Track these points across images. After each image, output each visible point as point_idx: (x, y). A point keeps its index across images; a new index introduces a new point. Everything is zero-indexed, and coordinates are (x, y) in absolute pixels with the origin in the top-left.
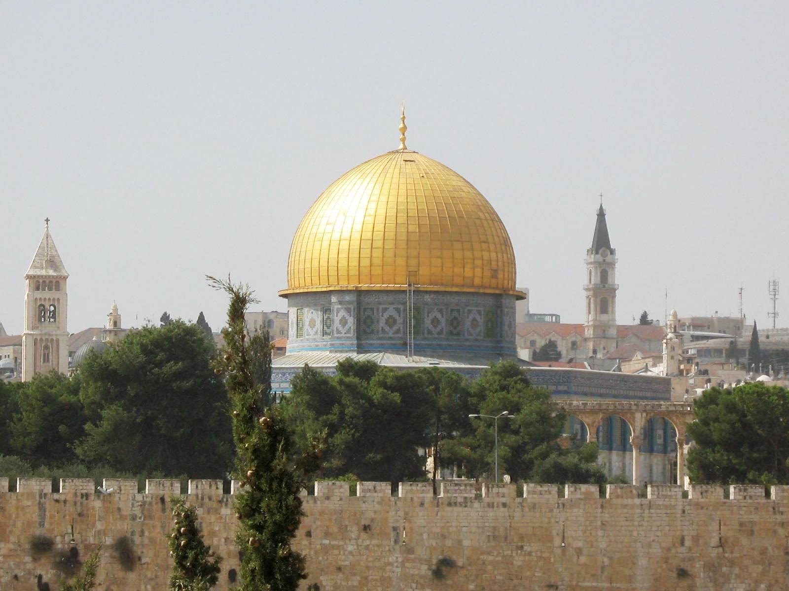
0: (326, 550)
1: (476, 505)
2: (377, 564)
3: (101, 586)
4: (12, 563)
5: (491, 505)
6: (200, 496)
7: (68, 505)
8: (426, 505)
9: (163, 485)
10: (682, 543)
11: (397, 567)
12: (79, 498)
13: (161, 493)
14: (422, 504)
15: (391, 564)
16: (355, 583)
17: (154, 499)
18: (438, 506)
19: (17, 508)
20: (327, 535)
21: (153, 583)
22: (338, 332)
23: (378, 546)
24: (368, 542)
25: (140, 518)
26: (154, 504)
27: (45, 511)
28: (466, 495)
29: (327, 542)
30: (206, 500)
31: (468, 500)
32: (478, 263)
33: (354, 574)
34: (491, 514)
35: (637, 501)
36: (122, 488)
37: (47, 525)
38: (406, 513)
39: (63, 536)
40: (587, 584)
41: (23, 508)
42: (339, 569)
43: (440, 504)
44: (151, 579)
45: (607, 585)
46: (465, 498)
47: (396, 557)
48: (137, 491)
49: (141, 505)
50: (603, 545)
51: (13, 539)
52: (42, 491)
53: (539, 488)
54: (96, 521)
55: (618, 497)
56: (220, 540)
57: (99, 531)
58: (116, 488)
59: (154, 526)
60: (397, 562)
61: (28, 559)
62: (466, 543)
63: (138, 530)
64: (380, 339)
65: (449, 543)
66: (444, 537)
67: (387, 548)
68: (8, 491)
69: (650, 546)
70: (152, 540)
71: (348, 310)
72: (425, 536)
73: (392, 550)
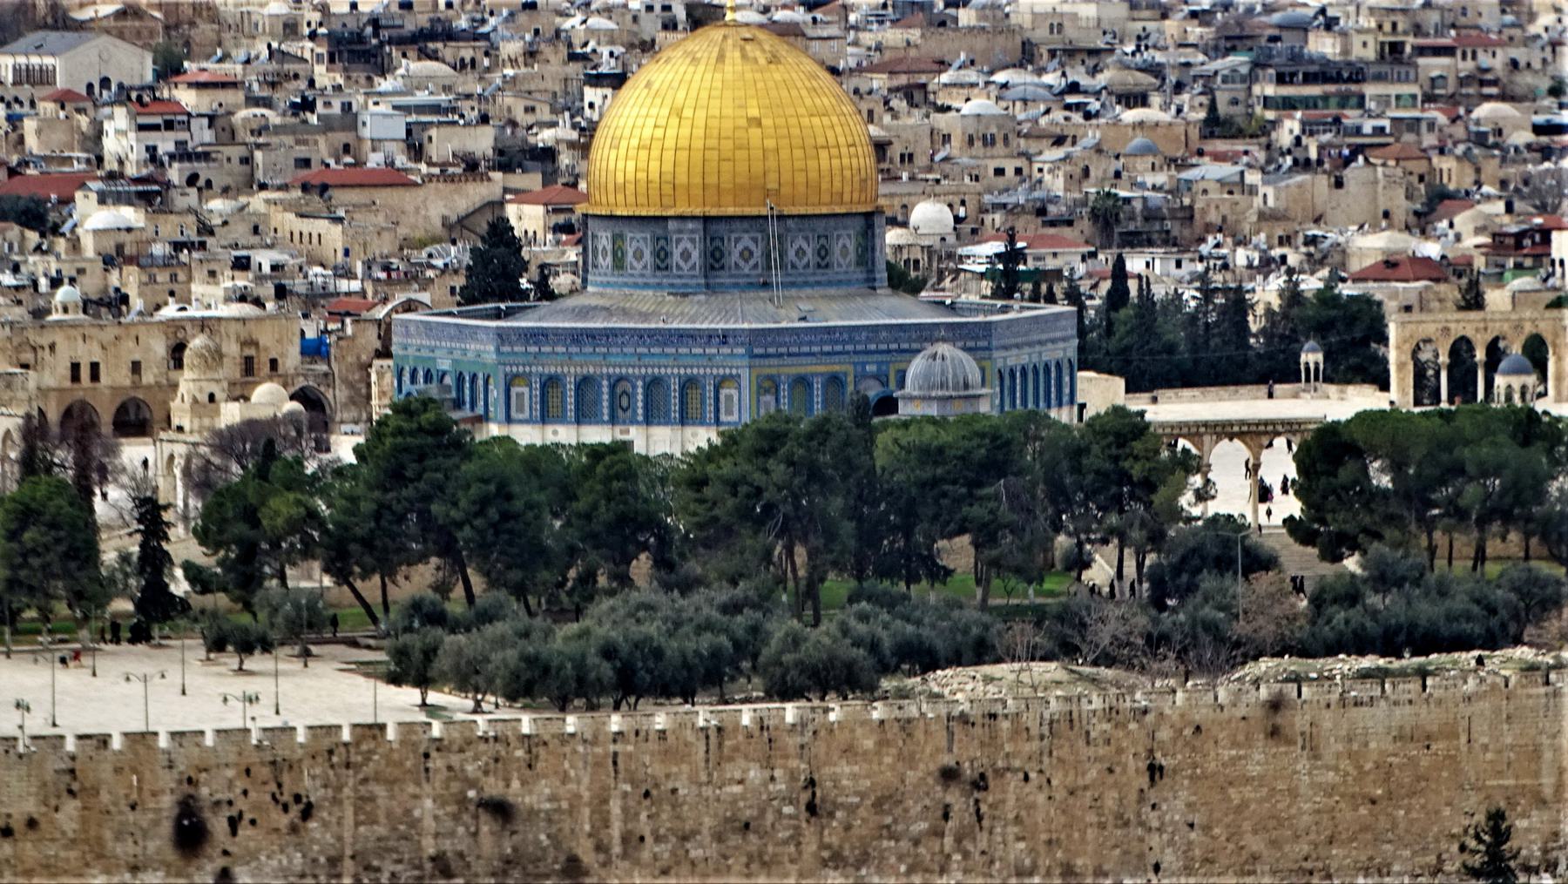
0: (1234, 760)
1: (1383, 703)
5: (1396, 703)
14: (1328, 706)
20: (1235, 744)
22: (679, 268)
29: (1234, 752)
34: (1398, 711)
35: (1542, 690)
40: (1494, 783)
47: (1303, 765)
50: (1509, 740)
51: (922, 766)
55: (1523, 687)
57: (1007, 755)
61: (939, 788)
62: (1373, 745)
64: (731, 276)
65: (1355, 747)
66: (1350, 740)
70: (1060, 760)
71: (693, 241)
72: (1332, 740)
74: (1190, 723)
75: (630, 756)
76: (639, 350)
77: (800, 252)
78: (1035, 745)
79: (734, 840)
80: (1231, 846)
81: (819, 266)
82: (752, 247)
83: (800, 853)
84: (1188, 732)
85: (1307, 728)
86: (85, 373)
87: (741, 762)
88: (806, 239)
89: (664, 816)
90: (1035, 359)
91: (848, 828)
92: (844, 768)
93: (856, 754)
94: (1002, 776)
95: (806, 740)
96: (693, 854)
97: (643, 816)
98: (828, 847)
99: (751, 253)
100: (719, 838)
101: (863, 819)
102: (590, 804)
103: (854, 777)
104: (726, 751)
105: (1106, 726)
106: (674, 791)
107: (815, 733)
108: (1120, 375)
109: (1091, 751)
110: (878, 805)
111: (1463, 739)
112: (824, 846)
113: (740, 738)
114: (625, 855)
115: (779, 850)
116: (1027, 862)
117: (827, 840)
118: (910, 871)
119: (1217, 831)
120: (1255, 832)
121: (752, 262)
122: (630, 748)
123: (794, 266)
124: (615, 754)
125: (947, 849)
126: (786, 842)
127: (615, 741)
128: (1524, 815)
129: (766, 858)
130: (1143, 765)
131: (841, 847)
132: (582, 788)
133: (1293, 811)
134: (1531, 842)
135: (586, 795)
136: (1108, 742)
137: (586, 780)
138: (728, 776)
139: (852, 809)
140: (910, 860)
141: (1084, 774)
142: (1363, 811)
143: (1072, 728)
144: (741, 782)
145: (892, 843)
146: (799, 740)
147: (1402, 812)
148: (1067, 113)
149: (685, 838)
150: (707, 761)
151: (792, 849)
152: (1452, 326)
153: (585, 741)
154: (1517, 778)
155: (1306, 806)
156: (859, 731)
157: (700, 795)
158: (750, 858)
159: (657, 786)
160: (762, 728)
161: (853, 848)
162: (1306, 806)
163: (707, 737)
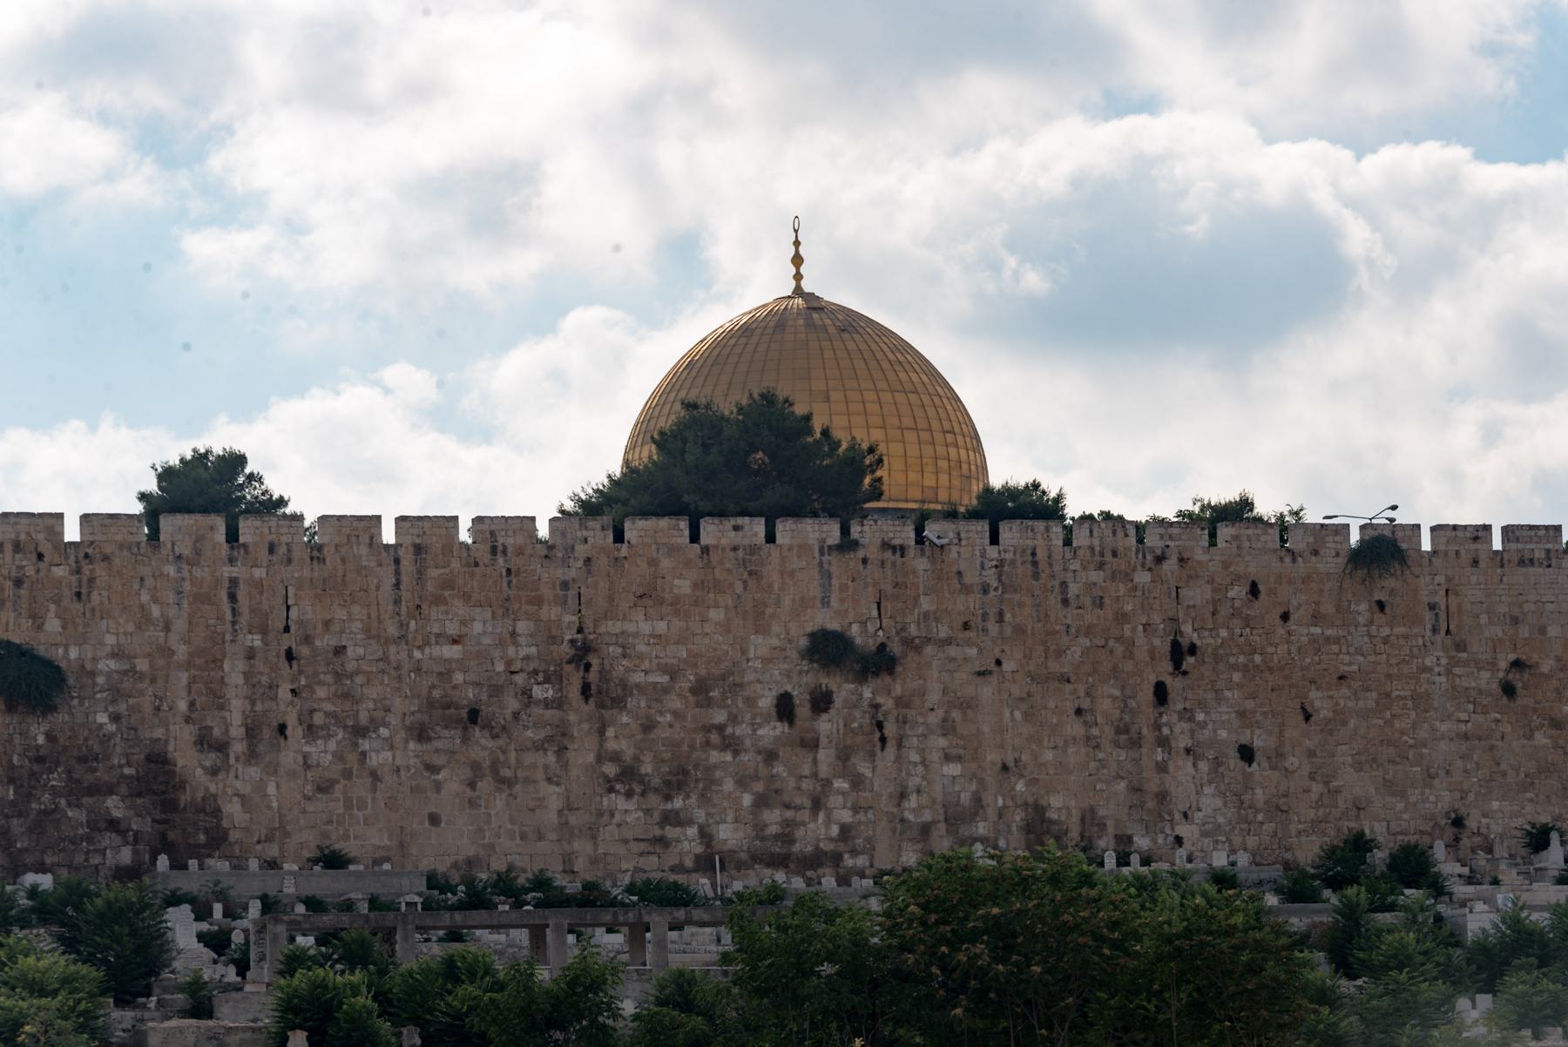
0: (1317, 644)
2: (1406, 669)
3: (933, 713)
4: (777, 672)
6: (1097, 549)
7: (869, 567)
8: (1482, 564)
9: (1032, 530)
11: (1439, 674)
13: (1030, 542)
14: (1475, 562)
15: (1430, 670)
16: (1371, 704)
17: (1018, 555)
18: (1502, 566)
19: (782, 573)
20: (1316, 618)
21: (1024, 706)
23: (1406, 637)
24: (1386, 631)
25: (996, 589)
26: (1018, 564)
27: (830, 578)
28: (1549, 546)
29: (1318, 630)
30: (1109, 557)
31: (1553, 555)
32: (943, 464)
33: (1368, 690)
36: (963, 535)
37: (834, 603)
38: (1449, 579)
39: (863, 623)
41: (792, 574)
43: (1505, 561)
44: (1021, 699)
46: (1548, 551)
48: (987, 541)
49: (996, 567)
51: (776, 628)
52: (824, 540)
54: (919, 596)
56: (1134, 630)
57: (926, 615)
58: (951, 535)
59: (1021, 605)
60: (1438, 665)
62: (1553, 631)
63: (993, 612)
65: (1524, 632)
66: (1515, 621)
67: (1420, 641)
68: (764, 540)
70: (1019, 630)
72: (1484, 619)
73: (1428, 644)
74: (1238, 578)
75: (259, 586)
78: (973, 601)
79: (448, 738)
80: (1317, 788)
83: (565, 766)
84: (1239, 592)
85: (1440, 599)
87: (459, 608)
89: (321, 692)
91: (648, 727)
92: (641, 625)
93: (661, 602)
94: (918, 649)
95: (572, 573)
96: (374, 760)
97: (284, 693)
98: (615, 758)
100: (421, 734)
101: (675, 713)
102: (189, 665)
104: (430, 587)
105: (1096, 576)
106: (339, 650)
109: (1070, 616)
110: (700, 690)
114: (252, 755)
115: (529, 758)
116: (965, 798)
117: (611, 745)
118: (761, 802)
119: (1292, 761)
120: (1358, 767)
122: (259, 573)
124: (234, 582)
125: (824, 770)
126: (540, 747)
129: (506, 772)
130: (1162, 645)
131: (636, 759)
132: (173, 638)
133: (1423, 733)
135: (182, 651)
136: (1099, 603)
137: (180, 625)
138: (436, 629)
139: (657, 694)
140: (759, 787)
141: (1060, 653)
142: (1541, 739)
143: (1036, 576)
145: (728, 757)
146: (559, 573)
149: (359, 732)
150: (397, 602)
151: (551, 758)
156: (666, 563)
157: (385, 659)
158: (476, 766)
159: (307, 640)
160: (494, 551)
161: (658, 761)
162: (1443, 727)
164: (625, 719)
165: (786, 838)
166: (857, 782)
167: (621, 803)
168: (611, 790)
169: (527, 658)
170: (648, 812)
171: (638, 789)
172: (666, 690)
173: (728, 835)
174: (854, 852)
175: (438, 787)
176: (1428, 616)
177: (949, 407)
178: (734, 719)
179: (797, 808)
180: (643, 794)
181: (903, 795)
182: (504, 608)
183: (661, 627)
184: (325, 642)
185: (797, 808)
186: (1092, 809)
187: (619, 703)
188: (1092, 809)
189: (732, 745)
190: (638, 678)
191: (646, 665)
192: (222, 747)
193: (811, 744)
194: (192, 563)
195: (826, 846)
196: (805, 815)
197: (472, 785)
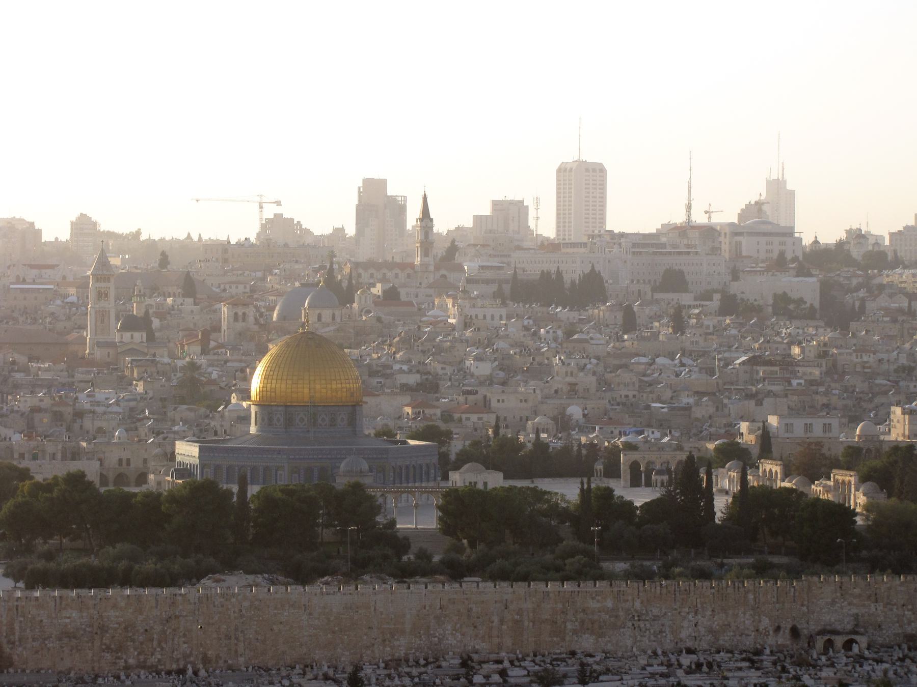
1: (339, 594)
10: (425, 608)
12: (172, 596)
14: (316, 595)
20: (276, 608)
22: (276, 425)
24: (293, 611)
29: (276, 611)
30: (225, 596)
35: (406, 591)
40: (385, 626)
42: (281, 623)
45: (393, 626)
51: (145, 613)
53: (365, 586)
62: (334, 610)
65: (327, 610)
66: (325, 608)
69: (411, 609)
75: (23, 607)
76: (249, 456)
77: (323, 420)
79: (66, 640)
81: (331, 425)
82: (304, 417)
86: (124, 463)
88: (326, 414)
89: (37, 630)
90: (413, 463)
92: (112, 613)
94: (178, 618)
95: (96, 602)
96: (48, 645)
98: (105, 644)
99: (303, 420)
100: (60, 639)
101: (120, 634)
103: (116, 617)
105: (222, 600)
106: (42, 621)
107: (100, 599)
108: (500, 470)
110: (126, 628)
111: (373, 609)
112: (102, 644)
113: (69, 600)
116: (188, 652)
117: (104, 641)
118: (139, 654)
121: (304, 423)
122: (23, 603)
123: (320, 425)
124: (17, 606)
126: (87, 642)
127: (17, 601)
128: (398, 640)
129: (79, 648)
134: (401, 650)
135: (5, 622)
136: (222, 606)
137: (5, 616)
138: (64, 615)
140: (139, 650)
142: (329, 636)
143: (208, 600)
144: (68, 618)
145: (132, 643)
147: (346, 637)
148: (444, 366)
149: (45, 639)
150: (55, 609)
151: (90, 644)
152: (647, 456)
153: (5, 601)
154: (395, 625)
155: (306, 634)
156: (119, 599)
160: (78, 597)
163: (56, 600)
164: (108, 635)
165: (145, 662)
166: (162, 649)
167: (106, 654)
168: (104, 651)
169: (85, 622)
170: (112, 656)
171: (110, 651)
172: (118, 629)
173: (131, 661)
174: (161, 665)
175: (63, 651)
176: (303, 608)
177: (348, 371)
178: (134, 635)
179: (148, 655)
180: (111, 653)
181: (173, 652)
182: (81, 611)
183: (117, 614)
184: (38, 619)
185: (148, 655)
186: (219, 654)
187: (107, 631)
188: (219, 654)
189: (133, 641)
190: (112, 625)
191: (113, 623)
192: (13, 643)
193: (152, 640)
194: (8, 602)
195: (154, 664)
196: (149, 657)
197: (71, 651)
